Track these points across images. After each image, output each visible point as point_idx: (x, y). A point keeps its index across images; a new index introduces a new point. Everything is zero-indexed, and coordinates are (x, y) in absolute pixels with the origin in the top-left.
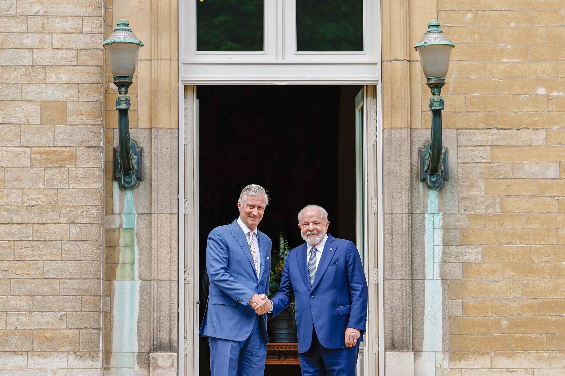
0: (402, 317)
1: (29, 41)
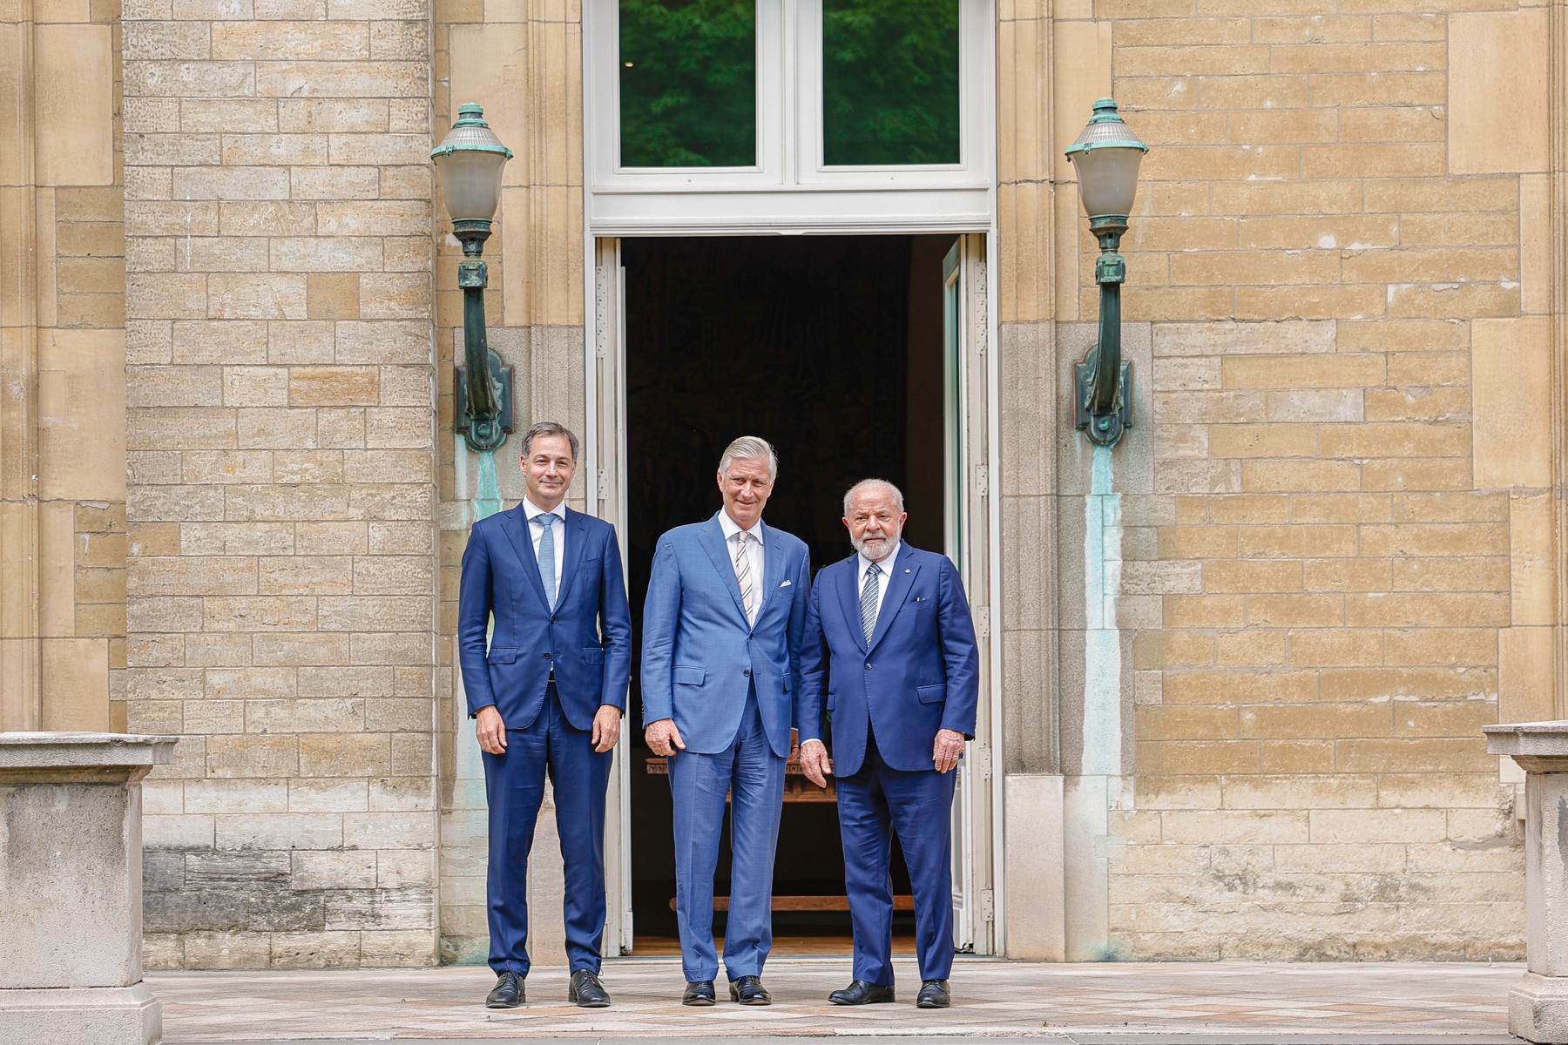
0: (1040, 705)
1: (282, 149)
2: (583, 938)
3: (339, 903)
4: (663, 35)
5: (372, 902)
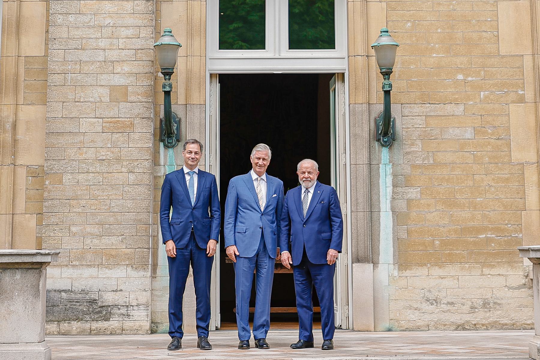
1: (102, 44)
2: (203, 325)
3: (115, 311)
4: (234, 3)
5: (127, 310)
